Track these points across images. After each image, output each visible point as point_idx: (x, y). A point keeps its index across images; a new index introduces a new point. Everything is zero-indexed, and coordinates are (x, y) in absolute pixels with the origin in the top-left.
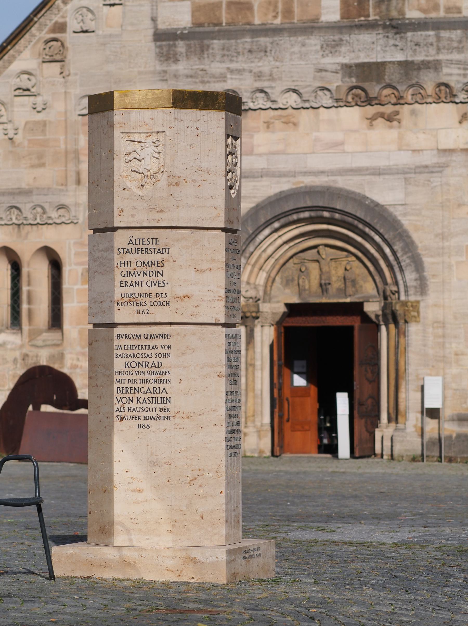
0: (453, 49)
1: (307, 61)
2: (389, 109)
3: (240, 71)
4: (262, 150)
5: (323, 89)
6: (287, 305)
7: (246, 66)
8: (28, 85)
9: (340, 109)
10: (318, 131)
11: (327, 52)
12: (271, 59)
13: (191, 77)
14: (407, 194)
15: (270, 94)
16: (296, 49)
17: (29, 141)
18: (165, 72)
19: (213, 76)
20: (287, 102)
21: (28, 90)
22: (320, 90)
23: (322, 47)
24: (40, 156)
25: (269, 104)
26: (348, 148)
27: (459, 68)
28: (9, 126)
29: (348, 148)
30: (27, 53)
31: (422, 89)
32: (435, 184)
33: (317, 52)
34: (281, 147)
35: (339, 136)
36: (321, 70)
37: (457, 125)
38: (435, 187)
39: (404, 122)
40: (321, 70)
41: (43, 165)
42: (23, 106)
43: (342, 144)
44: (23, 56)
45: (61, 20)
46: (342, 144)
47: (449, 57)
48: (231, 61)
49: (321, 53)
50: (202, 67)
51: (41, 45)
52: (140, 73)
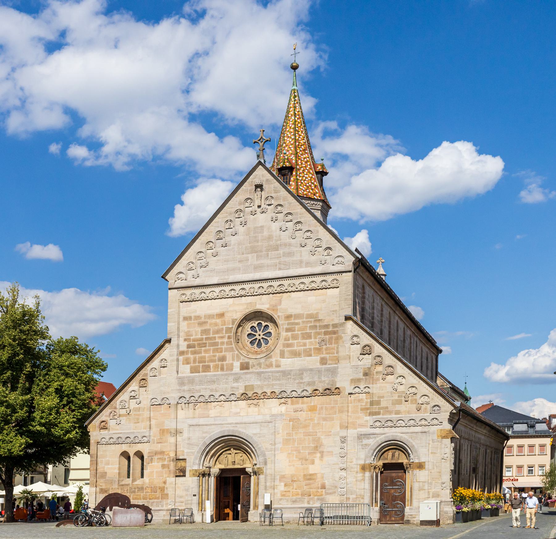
2: (255, 402)
3: (206, 389)
4: (212, 416)
5: (233, 394)
6: (220, 469)
7: (207, 387)
8: (134, 395)
13: (189, 391)
16: (224, 381)
17: (134, 414)
19: (197, 391)
21: (134, 397)
24: (138, 419)
25: (215, 400)
26: (241, 414)
28: (128, 409)
29: (241, 414)
30: (134, 384)
33: (231, 381)
34: (219, 415)
35: (238, 410)
36: (233, 388)
40: (233, 388)
41: (139, 422)
42: (132, 402)
44: (133, 385)
45: (146, 372)
46: (239, 413)
48: (203, 385)
51: (138, 381)
52: (172, 390)
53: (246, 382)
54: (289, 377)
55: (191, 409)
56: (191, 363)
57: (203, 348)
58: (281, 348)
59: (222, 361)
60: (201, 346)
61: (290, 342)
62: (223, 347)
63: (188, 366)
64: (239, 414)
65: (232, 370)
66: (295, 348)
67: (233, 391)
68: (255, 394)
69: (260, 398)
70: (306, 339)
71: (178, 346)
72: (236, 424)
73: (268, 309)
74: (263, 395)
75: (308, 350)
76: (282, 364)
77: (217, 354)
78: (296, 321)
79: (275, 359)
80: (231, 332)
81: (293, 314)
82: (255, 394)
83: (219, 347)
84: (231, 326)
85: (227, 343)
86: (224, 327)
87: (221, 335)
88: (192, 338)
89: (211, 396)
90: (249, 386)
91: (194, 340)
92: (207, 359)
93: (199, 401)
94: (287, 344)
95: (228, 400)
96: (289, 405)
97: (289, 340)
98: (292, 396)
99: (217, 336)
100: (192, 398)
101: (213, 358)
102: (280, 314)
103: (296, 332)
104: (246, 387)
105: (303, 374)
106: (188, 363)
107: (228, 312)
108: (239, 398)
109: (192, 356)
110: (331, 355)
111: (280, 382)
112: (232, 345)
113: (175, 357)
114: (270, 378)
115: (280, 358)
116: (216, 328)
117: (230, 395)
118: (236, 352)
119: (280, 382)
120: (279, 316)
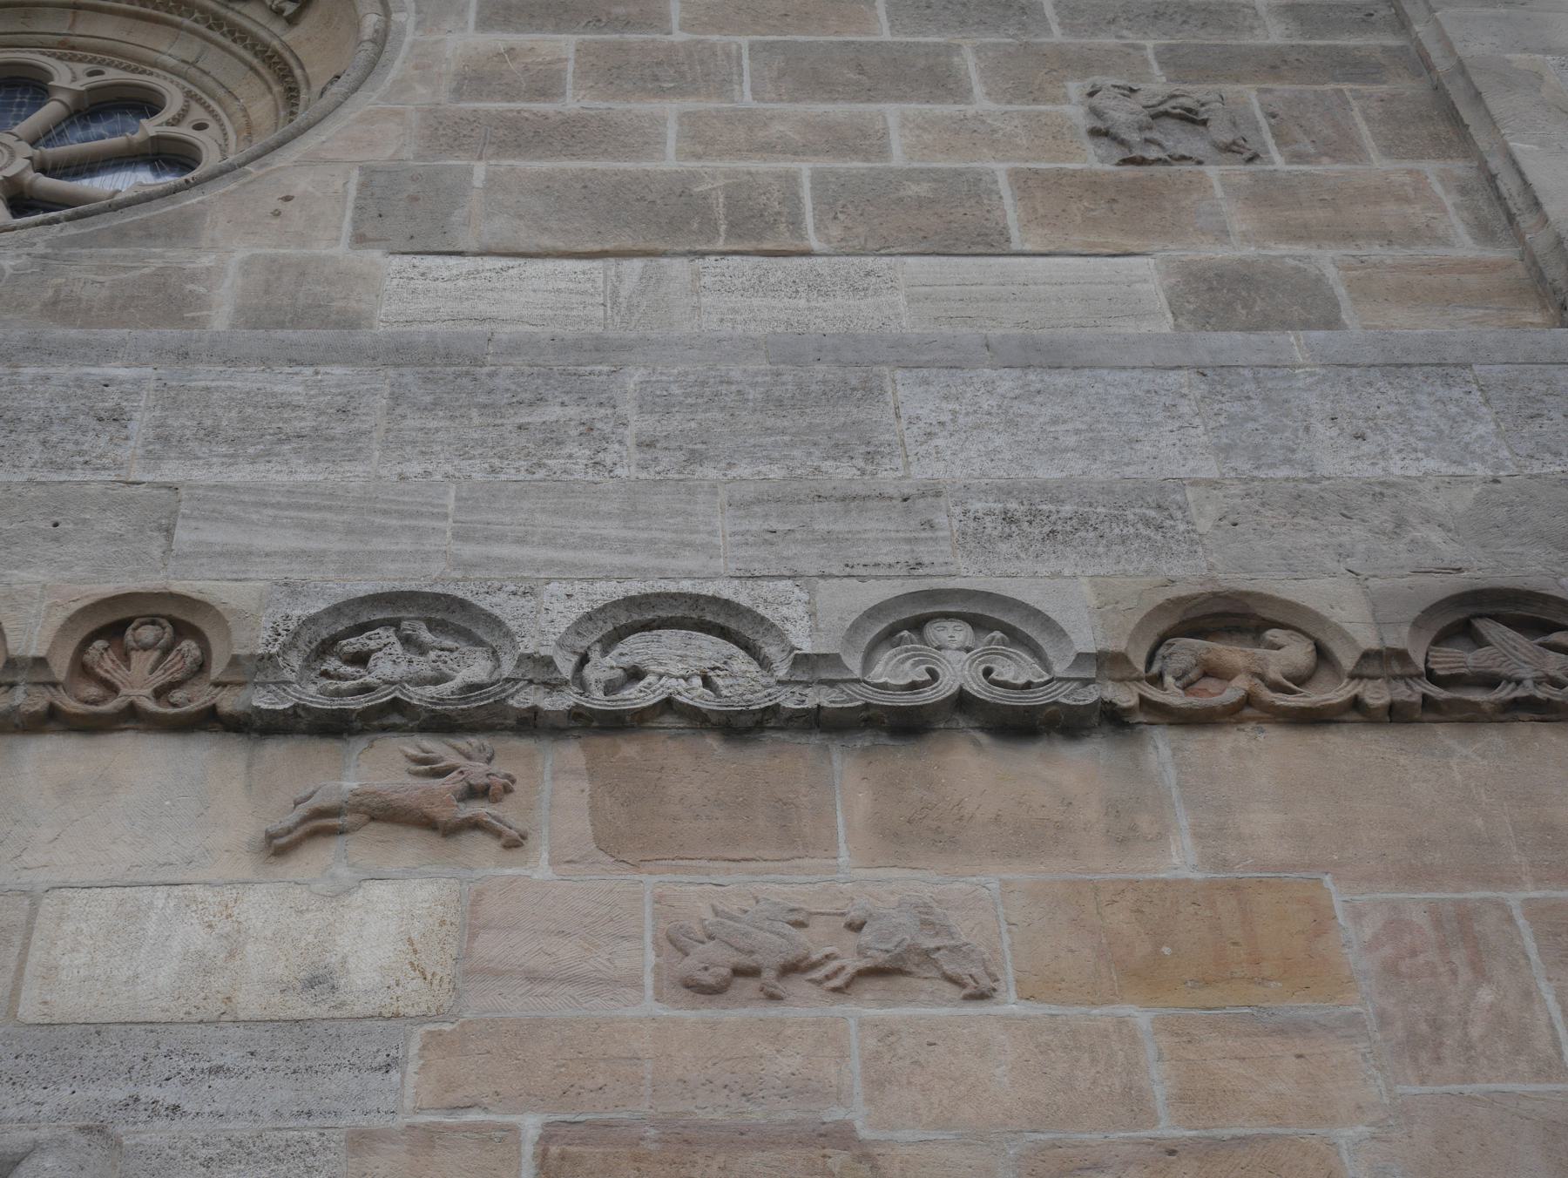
0: (280, 441)
47: (241, 474)
54: (553, 413)
70: (869, 94)
75: (922, 189)
79: (241, 254)
96: (539, 867)
98: (636, 697)
103: (679, 37)
105: (870, 391)
110: (1376, 251)
114: (117, 417)
115: (360, 239)
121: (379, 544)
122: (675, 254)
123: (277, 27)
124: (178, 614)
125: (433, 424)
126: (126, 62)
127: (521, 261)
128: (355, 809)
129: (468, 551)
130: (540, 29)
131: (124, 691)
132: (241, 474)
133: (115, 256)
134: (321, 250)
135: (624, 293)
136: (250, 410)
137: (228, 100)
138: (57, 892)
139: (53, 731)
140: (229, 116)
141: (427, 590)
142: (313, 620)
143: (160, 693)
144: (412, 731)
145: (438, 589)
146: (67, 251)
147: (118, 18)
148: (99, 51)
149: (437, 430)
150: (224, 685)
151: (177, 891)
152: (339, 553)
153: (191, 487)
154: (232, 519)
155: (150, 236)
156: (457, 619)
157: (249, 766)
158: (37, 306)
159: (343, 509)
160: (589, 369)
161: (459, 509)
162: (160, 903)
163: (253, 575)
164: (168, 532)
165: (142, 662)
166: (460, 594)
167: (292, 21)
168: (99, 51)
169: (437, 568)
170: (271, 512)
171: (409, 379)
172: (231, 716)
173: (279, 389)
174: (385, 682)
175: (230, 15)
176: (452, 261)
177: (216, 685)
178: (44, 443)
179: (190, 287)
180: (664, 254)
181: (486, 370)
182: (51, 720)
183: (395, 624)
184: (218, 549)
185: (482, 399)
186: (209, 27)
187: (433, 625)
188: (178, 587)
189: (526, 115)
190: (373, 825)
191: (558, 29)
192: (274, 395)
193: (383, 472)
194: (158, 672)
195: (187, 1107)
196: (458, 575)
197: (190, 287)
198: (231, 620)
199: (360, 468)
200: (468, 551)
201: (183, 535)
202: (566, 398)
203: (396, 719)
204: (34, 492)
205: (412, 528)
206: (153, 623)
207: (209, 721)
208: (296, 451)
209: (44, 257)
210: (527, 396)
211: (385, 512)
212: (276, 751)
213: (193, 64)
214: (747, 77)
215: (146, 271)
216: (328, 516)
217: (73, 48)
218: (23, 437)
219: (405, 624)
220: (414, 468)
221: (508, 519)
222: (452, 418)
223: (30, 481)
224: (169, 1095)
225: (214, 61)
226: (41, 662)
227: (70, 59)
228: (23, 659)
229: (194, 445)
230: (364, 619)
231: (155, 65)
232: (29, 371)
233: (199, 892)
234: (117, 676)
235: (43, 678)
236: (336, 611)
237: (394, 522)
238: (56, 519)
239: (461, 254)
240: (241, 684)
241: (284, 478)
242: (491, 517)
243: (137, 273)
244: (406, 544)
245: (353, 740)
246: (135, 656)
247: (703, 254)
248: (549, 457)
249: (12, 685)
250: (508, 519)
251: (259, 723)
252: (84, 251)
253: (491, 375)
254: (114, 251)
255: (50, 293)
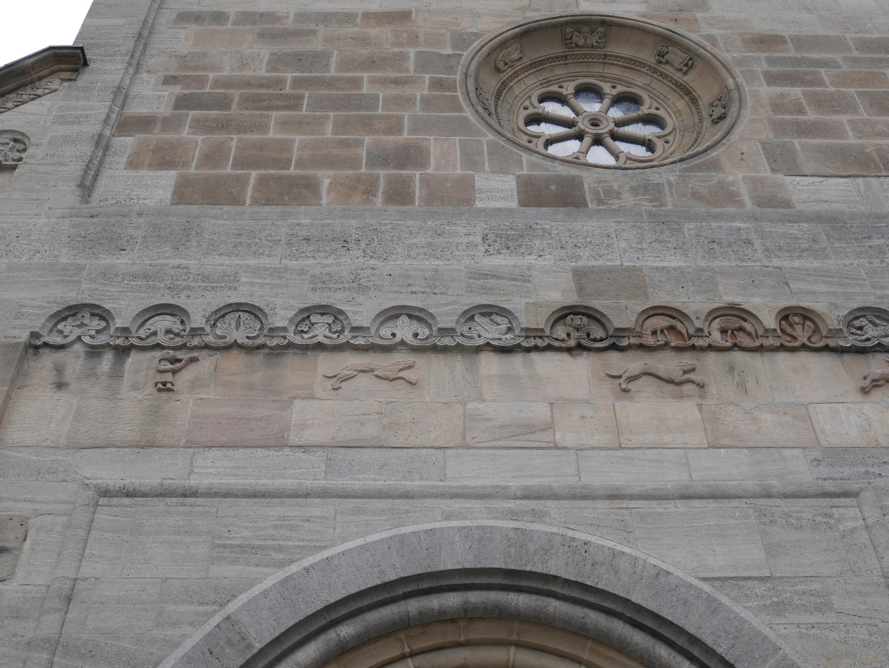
0: (803, 251)
1: (448, 260)
3: (278, 272)
4: (311, 435)
5: (489, 311)
7: (291, 264)
9: (534, 356)
10: (481, 398)
11: (497, 246)
12: (360, 253)
13: (146, 277)
14: (772, 550)
15: (350, 315)
16: (420, 240)
18: (80, 268)
19: (206, 278)
20: (394, 335)
22: (483, 314)
23: (485, 238)
25: (347, 336)
27: (830, 284)
31: (745, 320)
32: (850, 524)
34: (369, 431)
35: (539, 411)
37: (859, 397)
38: (852, 531)
39: (713, 389)
43: (549, 427)
46: (549, 427)
47: (797, 264)
49: (482, 249)
50: (177, 262)
53: (585, 253)
54: (876, 242)
55: (135, 387)
56: (186, 164)
57: (274, 114)
58: (767, 134)
59: (402, 167)
60: (265, 103)
61: (811, 116)
62: (406, 115)
63: (169, 177)
64: (546, 437)
65: (469, 201)
66: (852, 140)
67: (487, 290)
68: (661, 322)
69: (699, 342)
71: (121, 94)
72: (530, 495)
73: (644, 16)
74: (716, 324)
76: (794, 198)
77: (367, 139)
78: (814, 56)
79: (740, 176)
80: (450, 69)
81: (785, 34)
82: (661, 322)
83: (380, 111)
84: (449, 51)
85: (427, 102)
86: (412, 52)
87: (392, 74)
88: (211, 75)
89: (314, 319)
90: (611, 270)
91: (228, 83)
92: (295, 154)
93: (210, 339)
94: (797, 124)
95: (447, 341)
97: (801, 111)
99: (365, 75)
100: (162, 323)
101: (336, 151)
102: (716, 32)
103: (832, 89)
104: (579, 275)
106: (165, 164)
107: (429, 11)
108: (537, 333)
109: (200, 138)
111: (831, 263)
112: (460, 110)
113: (92, 128)
114: (749, 242)
115: (773, 170)
116: (365, 52)
117: (469, 316)
118: (491, 137)
119: (831, 263)
120: (711, 39)
121: (851, 290)
122: (871, 176)
123: (680, 74)
124: (803, 313)
125: (844, 245)
126: (624, 83)
127: (825, 179)
128: (883, 379)
129: (878, 292)
130: (786, 85)
131: (800, 339)
132: (797, 264)
133: (702, 176)
134: (762, 174)
135: (862, 191)
136: (787, 240)
137: (666, 100)
138: (811, 405)
139: (781, 351)
140: (668, 106)
141: (873, 306)
142: (845, 316)
143: (809, 339)
144: (883, 352)
145: (876, 306)
146: (687, 174)
147: (619, 68)
148: (617, 79)
149: (846, 248)
150: (828, 337)
151: (844, 405)
152: (841, 293)
153: (785, 268)
154: (803, 280)
155: (709, 168)
156: (882, 315)
157: (842, 363)
158: (689, 195)
159: (833, 277)
160: (879, 225)
161: (867, 277)
162: (841, 409)
163: (820, 300)
164: (787, 284)
165: (799, 328)
166: (884, 308)
167: (685, 73)
168: (617, 79)
169: (872, 298)
170: (813, 277)
171: (827, 228)
172: (833, 347)
173: (791, 231)
174: (873, 337)
175: (661, 69)
176: (804, 178)
177: (825, 337)
178: (733, 251)
179: (731, 188)
180: (867, 176)
181: (849, 225)
182: (782, 348)
183: (864, 316)
184: (805, 291)
185: (853, 236)
186: (652, 72)
187: (877, 317)
188: (802, 304)
189: (799, 121)
190: (887, 384)
191: (793, 86)
192: (791, 234)
193: (838, 263)
194: (805, 333)
195: (883, 474)
196: (879, 301)
197: (731, 188)
198: (823, 316)
199: (831, 262)
200: (878, 292)
201: (791, 285)
202: (878, 236)
203: (878, 348)
204: (741, 270)
205: (858, 284)
206: (796, 316)
207: (826, 349)
208: (809, 255)
209: (681, 176)
210: (865, 235)
211: (847, 278)
212: (848, 358)
213: (649, 85)
214: (861, 106)
215: (715, 182)
216: (831, 279)
217: (605, 77)
218: (726, 249)
219: (868, 317)
220: (847, 262)
221: (883, 281)
222: (848, 243)
223: (737, 265)
224: (876, 470)
225: (656, 84)
226: (775, 330)
227: (604, 81)
228: (770, 329)
229: (777, 253)
230: (856, 315)
231: (634, 85)
232: (714, 224)
233: (851, 405)
234: (794, 334)
235: (776, 335)
236: (850, 313)
237: (851, 282)
238: (753, 280)
239: (806, 176)
240: (832, 337)
241: (810, 265)
242: (879, 280)
243: (713, 182)
244: (858, 290)
245: (867, 354)
246: (795, 326)
247: (880, 177)
248: (884, 258)
249: (767, 337)
250: (883, 281)
251: (840, 349)
252: (692, 174)
253: (851, 227)
254: (701, 174)
255: (690, 190)
